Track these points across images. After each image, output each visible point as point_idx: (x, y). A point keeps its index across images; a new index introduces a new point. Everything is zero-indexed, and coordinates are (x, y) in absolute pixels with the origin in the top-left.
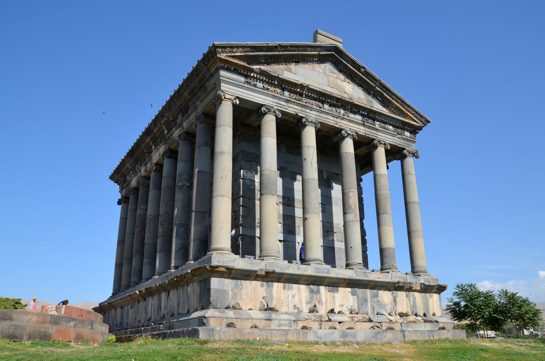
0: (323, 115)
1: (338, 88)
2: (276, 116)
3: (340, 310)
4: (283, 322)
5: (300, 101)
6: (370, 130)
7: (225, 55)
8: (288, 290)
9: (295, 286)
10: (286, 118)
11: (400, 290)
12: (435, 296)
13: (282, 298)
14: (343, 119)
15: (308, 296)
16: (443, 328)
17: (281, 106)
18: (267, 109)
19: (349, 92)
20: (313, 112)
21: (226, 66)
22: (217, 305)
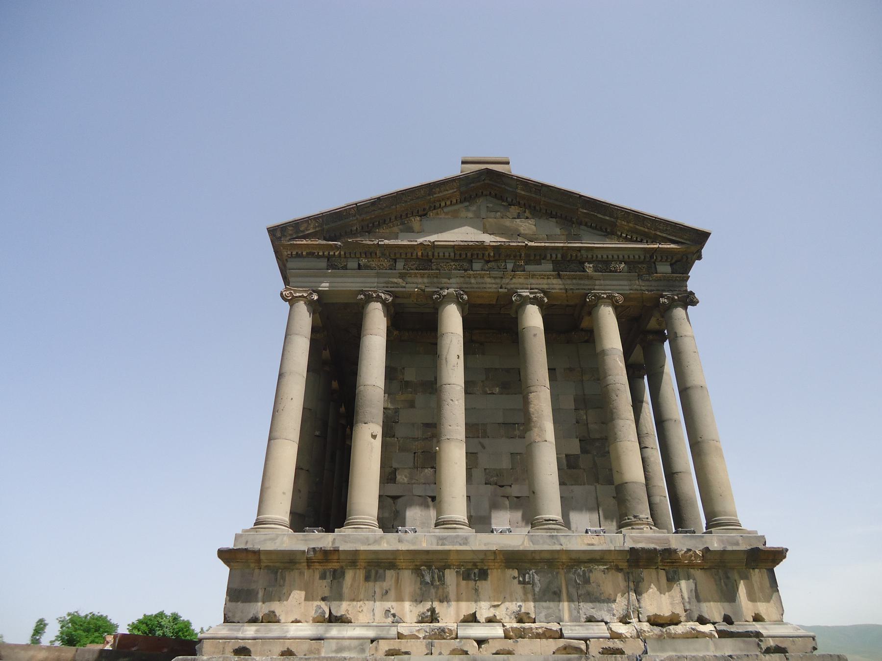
0: (473, 281)
2: (384, 302)
3: (491, 615)
4: (346, 643)
6: (574, 281)
8: (376, 580)
9: (390, 574)
10: (399, 301)
11: (647, 567)
12: (757, 576)
14: (514, 277)
15: (418, 591)
16: (779, 650)
18: (365, 295)
21: (294, 253)
22: (234, 616)
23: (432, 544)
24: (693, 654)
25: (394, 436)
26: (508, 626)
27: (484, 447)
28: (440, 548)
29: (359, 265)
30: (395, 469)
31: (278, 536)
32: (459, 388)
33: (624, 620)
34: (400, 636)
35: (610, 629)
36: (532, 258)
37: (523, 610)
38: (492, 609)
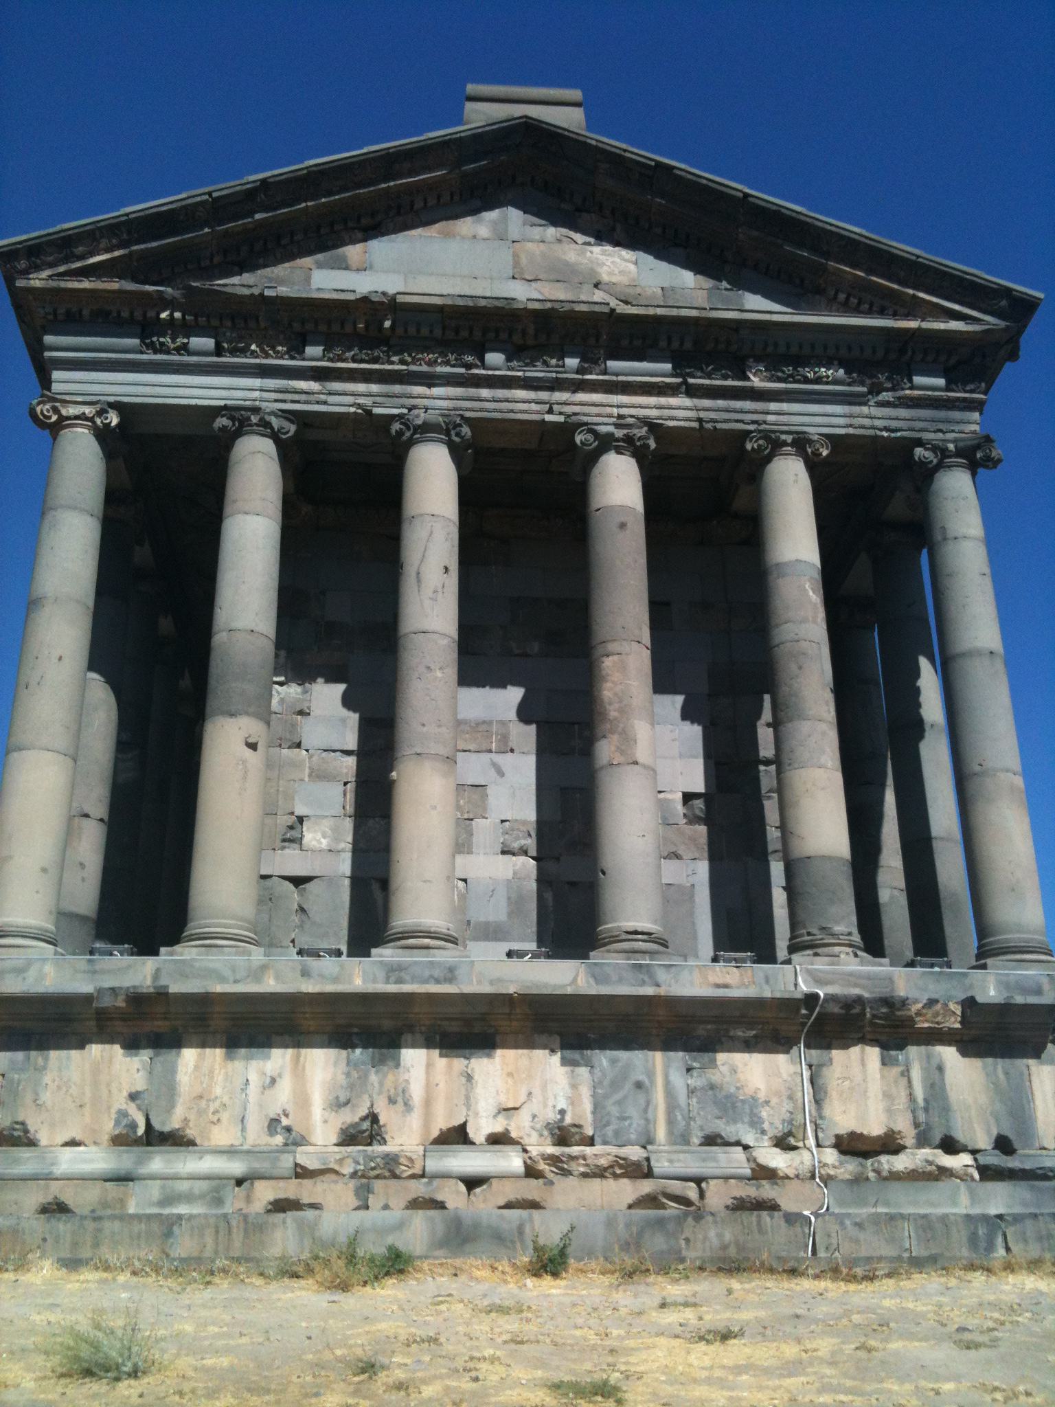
0: (485, 393)
1: (564, 273)
2: (275, 436)
3: (498, 1127)
4: (183, 1186)
5: (375, 360)
6: (721, 403)
7: (45, 274)
8: (248, 1058)
13: (218, 1091)
14: (579, 386)
15: (341, 1078)
17: (296, 397)
18: (232, 419)
19: (614, 280)
20: (436, 391)
21: (61, 311)
23: (374, 981)
24: (922, 1211)
25: (299, 745)
26: (534, 1151)
27: (501, 774)
28: (392, 988)
29: (218, 345)
30: (301, 820)
31: (29, 963)
32: (444, 642)
33: (783, 1143)
34: (301, 1173)
35: (751, 1159)
36: (625, 343)
37: (568, 1120)
38: (501, 1118)
